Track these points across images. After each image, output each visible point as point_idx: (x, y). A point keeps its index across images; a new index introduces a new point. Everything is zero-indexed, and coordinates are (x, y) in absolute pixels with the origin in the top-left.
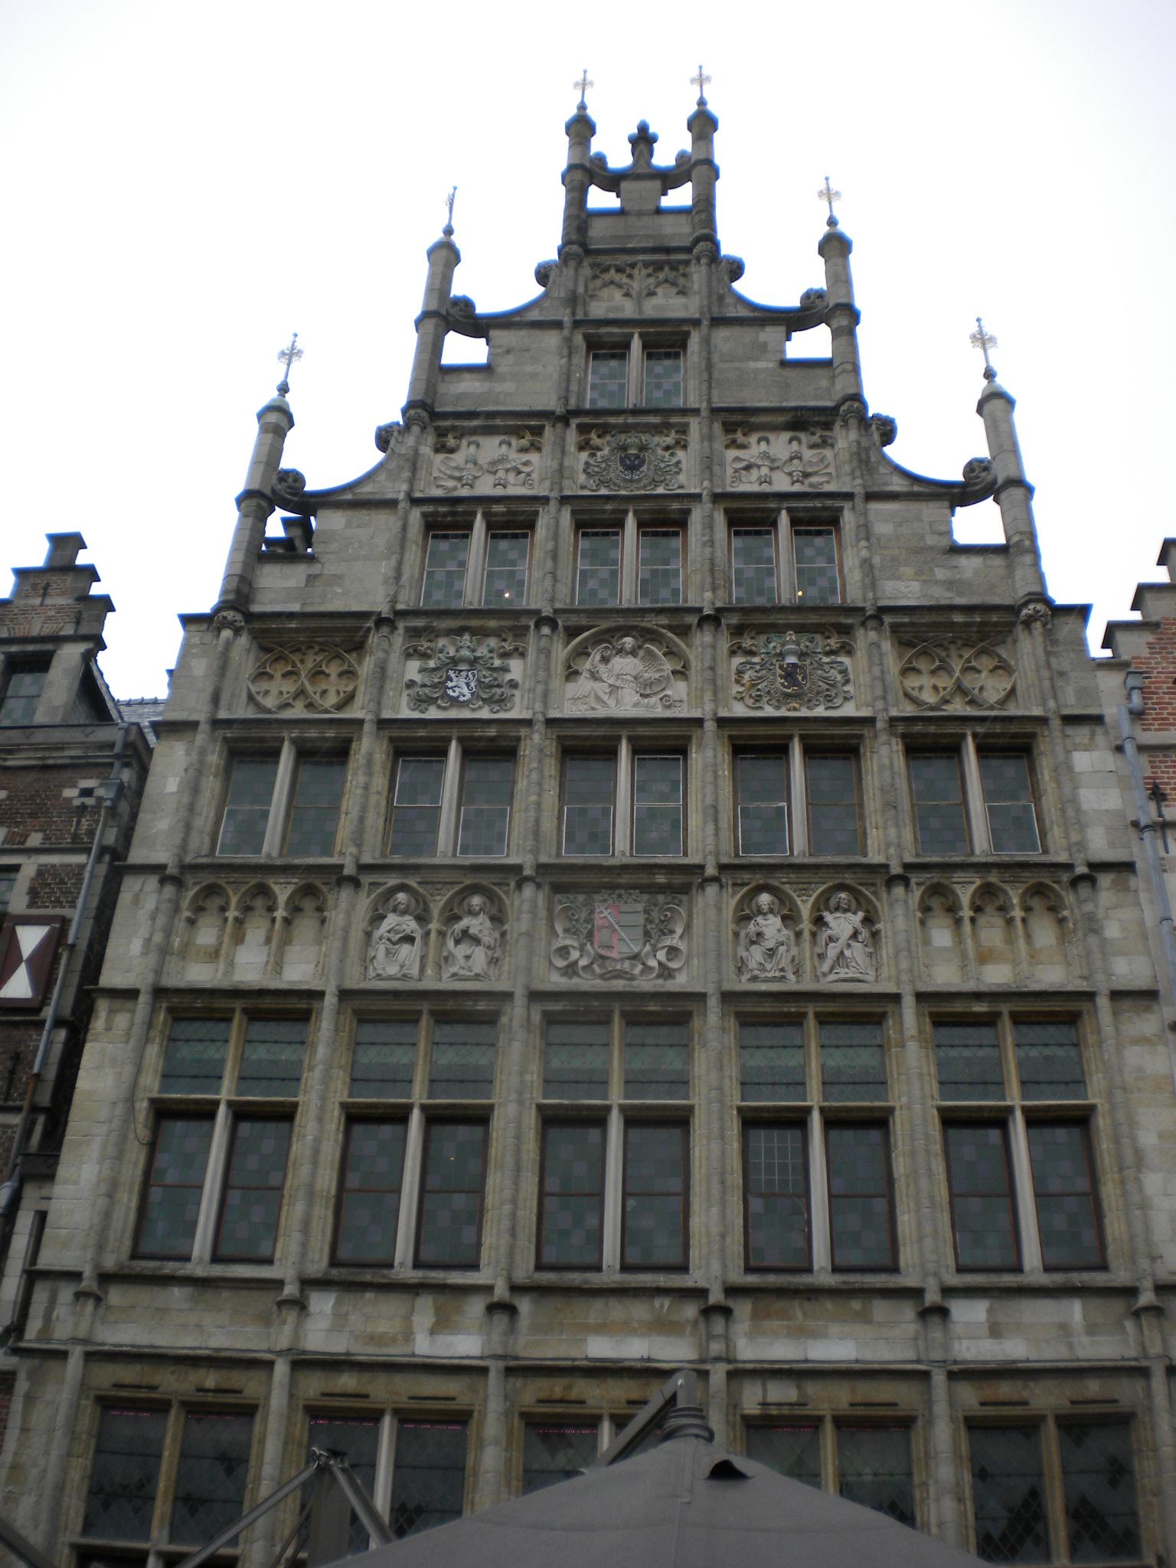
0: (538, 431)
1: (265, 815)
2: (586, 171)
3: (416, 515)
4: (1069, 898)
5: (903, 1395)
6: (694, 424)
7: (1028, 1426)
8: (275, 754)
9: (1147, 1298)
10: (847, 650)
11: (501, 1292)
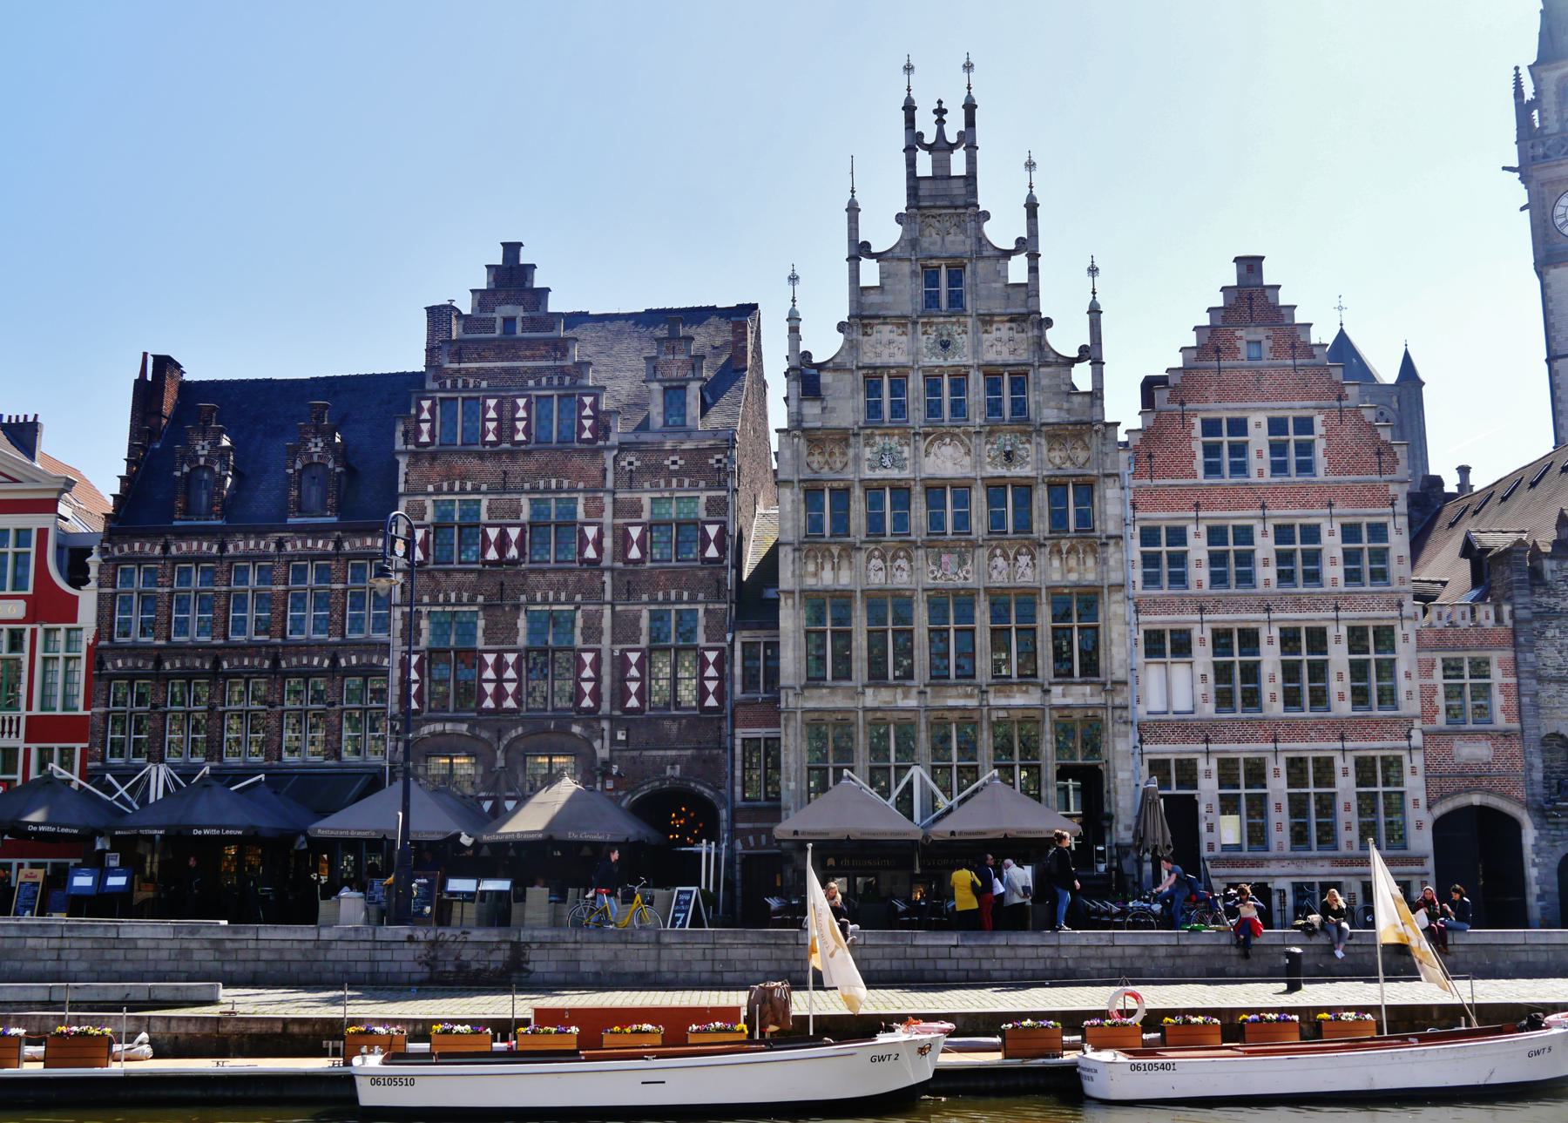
0: (905, 325)
1: (821, 516)
2: (914, 141)
3: (861, 374)
4: (1099, 549)
10: (1029, 442)
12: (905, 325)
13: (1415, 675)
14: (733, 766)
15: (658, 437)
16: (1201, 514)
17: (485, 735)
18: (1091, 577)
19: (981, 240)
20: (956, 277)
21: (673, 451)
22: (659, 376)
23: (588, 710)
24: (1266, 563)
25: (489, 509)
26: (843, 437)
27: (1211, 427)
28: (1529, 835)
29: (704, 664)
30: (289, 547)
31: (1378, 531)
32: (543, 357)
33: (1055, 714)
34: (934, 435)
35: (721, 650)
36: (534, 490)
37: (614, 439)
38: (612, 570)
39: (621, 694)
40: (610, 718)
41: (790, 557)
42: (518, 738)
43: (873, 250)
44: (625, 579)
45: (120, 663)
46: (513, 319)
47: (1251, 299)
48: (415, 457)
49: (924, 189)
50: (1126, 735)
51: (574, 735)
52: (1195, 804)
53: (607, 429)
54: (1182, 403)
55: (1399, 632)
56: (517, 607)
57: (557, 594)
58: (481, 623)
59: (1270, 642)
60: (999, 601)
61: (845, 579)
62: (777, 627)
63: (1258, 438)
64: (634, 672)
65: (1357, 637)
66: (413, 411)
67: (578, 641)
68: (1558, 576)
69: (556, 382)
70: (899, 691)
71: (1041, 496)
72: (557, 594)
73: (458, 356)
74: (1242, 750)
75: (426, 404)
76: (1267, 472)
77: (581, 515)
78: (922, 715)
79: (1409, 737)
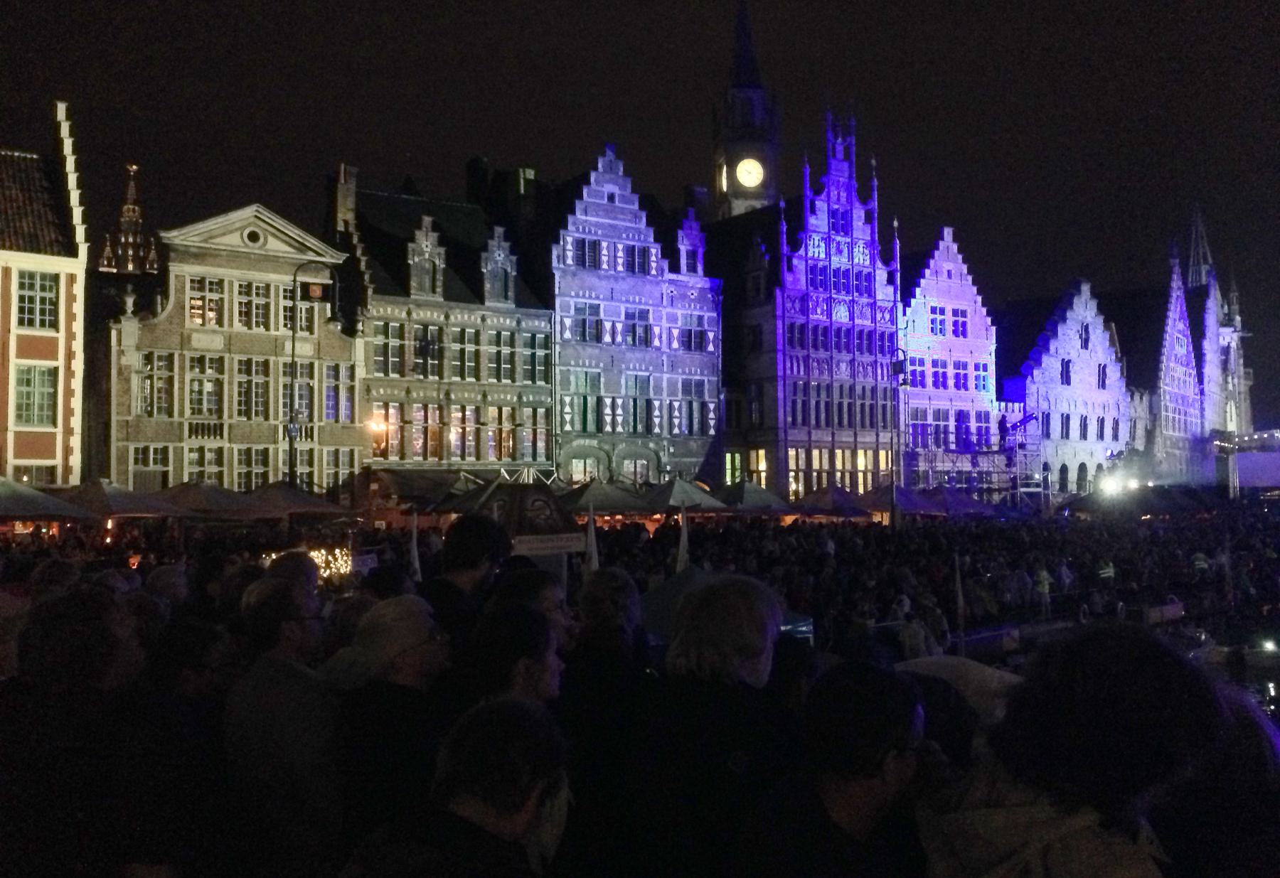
21: (692, 288)
36: (627, 301)
45: (382, 391)
48: (564, 271)
53: (663, 271)
56: (621, 372)
67: (652, 395)
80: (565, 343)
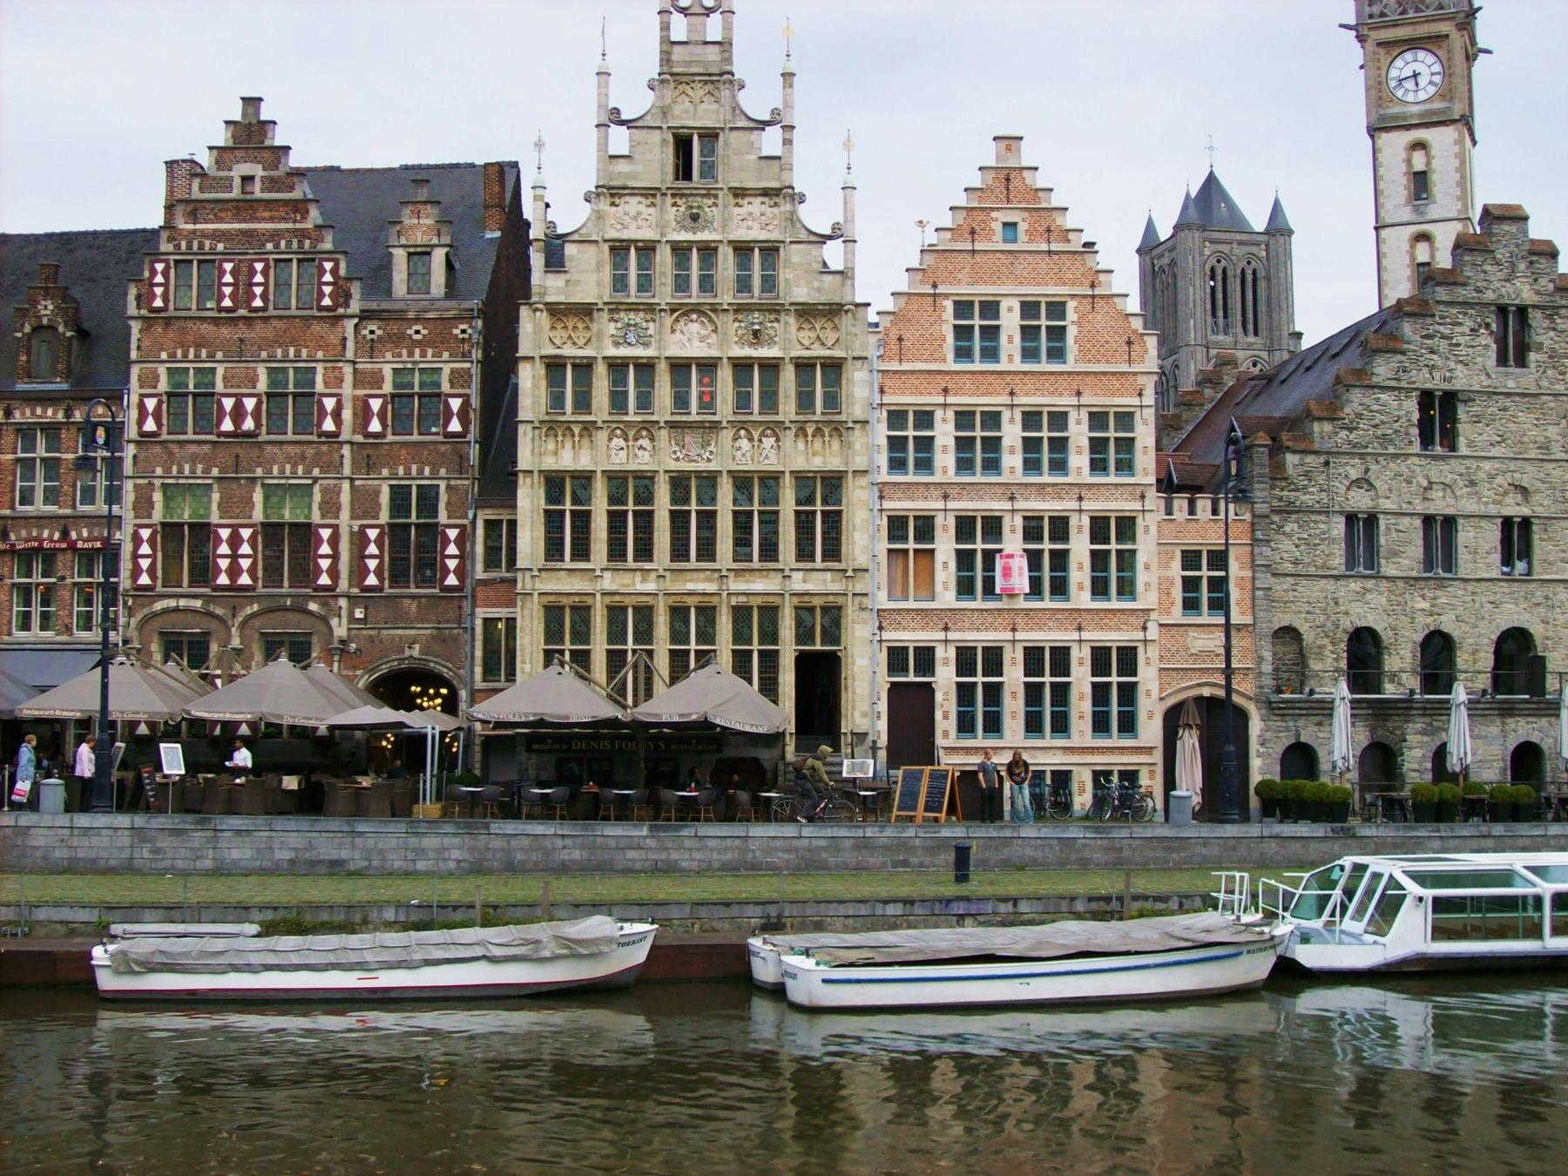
1: (563, 393)
3: (606, 247)
5: (776, 600)
6: (720, 193)
7: (812, 610)
8: (565, 366)
9: (850, 573)
10: (777, 320)
11: (661, 572)
12: (654, 196)
13: (1154, 565)
14: (473, 646)
15: (401, 306)
16: (950, 400)
17: (219, 611)
18: (835, 464)
19: (736, 109)
20: (709, 151)
21: (417, 320)
22: (403, 241)
23: (325, 588)
24: (1012, 452)
25: (225, 378)
26: (585, 311)
27: (963, 308)
28: (1255, 726)
29: (446, 541)
30: (17, 414)
31: (1125, 419)
32: (283, 219)
33: (795, 600)
34: (683, 311)
35: (462, 528)
37: (355, 307)
38: (351, 443)
39: (360, 571)
40: (349, 597)
41: (530, 435)
42: (253, 616)
43: (624, 117)
44: (365, 453)
46: (252, 178)
47: (1008, 180)
49: (678, 54)
50: (865, 622)
51: (311, 613)
52: (932, 691)
53: (348, 296)
54: (935, 286)
55: (1139, 521)
57: (294, 466)
58: (216, 496)
59: (1013, 531)
60: (742, 482)
61: (584, 462)
62: (514, 507)
63: (1010, 321)
64: (373, 549)
65: (1099, 529)
66: (147, 274)
68: (1300, 469)
69: (295, 245)
70: (638, 574)
71: (788, 376)
72: (294, 466)
73: (193, 217)
74: (980, 637)
75: (160, 267)
76: (1017, 357)
77: (320, 387)
78: (661, 598)
79: (1145, 628)
80: (145, 439)
